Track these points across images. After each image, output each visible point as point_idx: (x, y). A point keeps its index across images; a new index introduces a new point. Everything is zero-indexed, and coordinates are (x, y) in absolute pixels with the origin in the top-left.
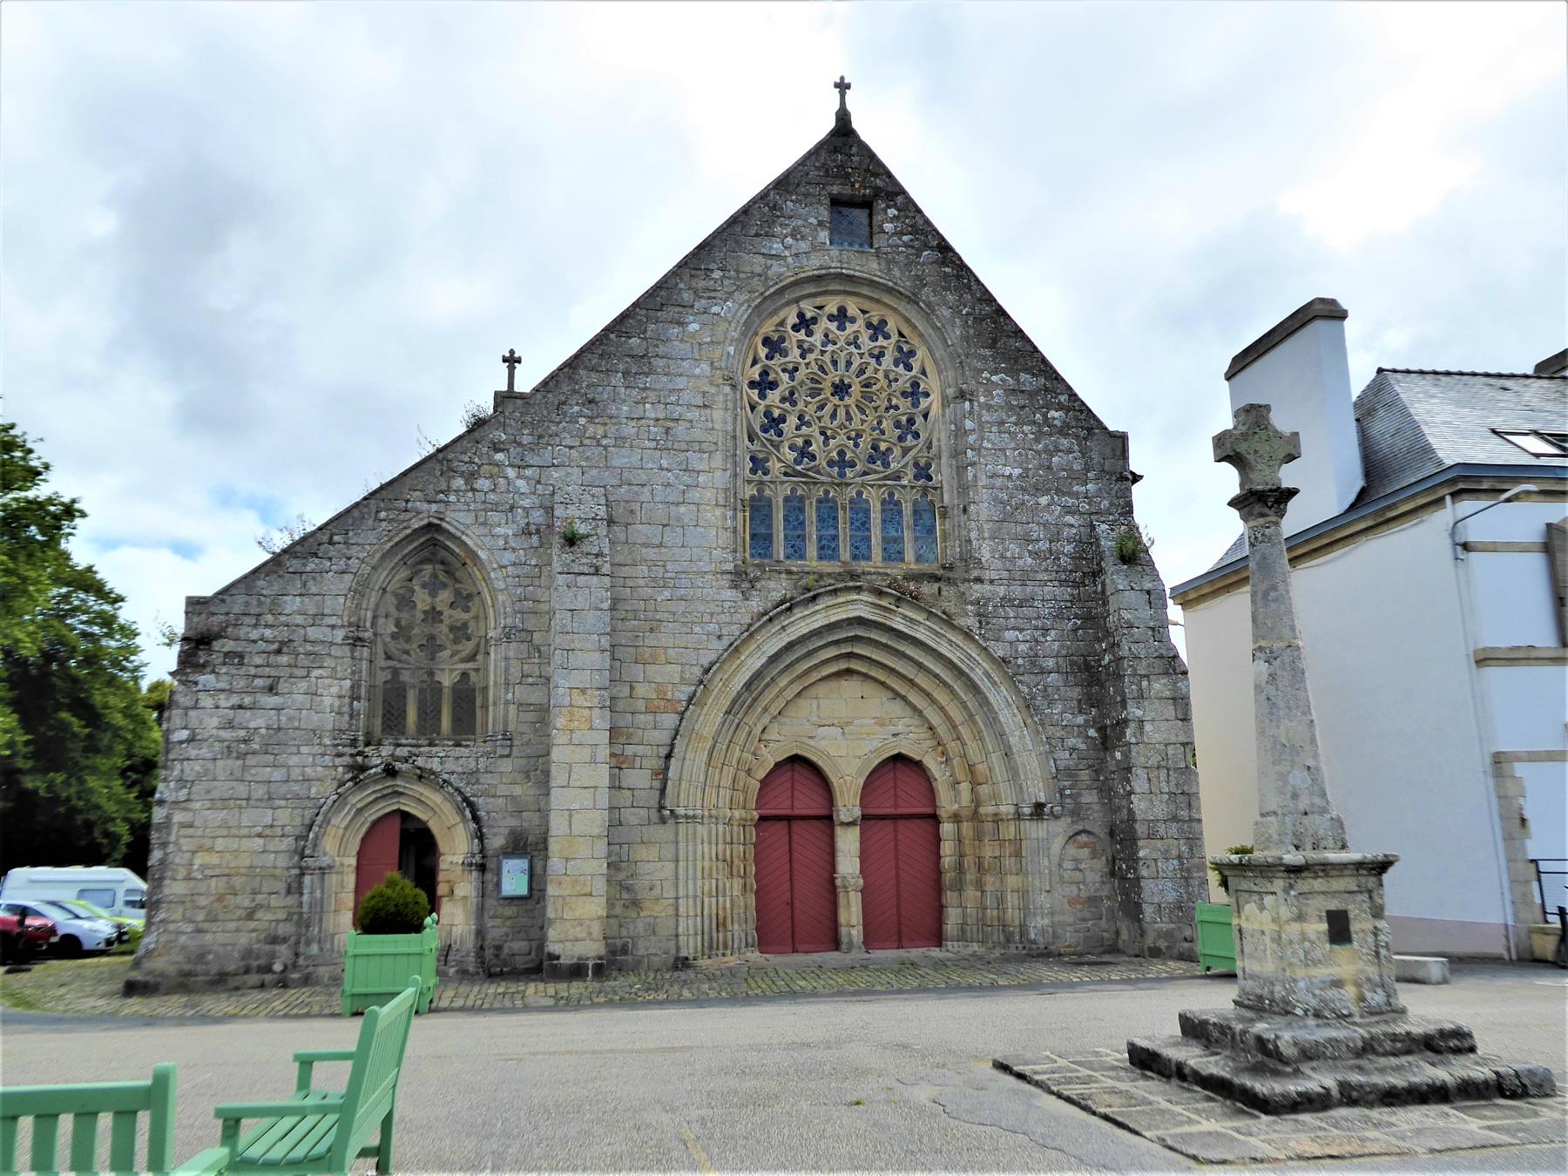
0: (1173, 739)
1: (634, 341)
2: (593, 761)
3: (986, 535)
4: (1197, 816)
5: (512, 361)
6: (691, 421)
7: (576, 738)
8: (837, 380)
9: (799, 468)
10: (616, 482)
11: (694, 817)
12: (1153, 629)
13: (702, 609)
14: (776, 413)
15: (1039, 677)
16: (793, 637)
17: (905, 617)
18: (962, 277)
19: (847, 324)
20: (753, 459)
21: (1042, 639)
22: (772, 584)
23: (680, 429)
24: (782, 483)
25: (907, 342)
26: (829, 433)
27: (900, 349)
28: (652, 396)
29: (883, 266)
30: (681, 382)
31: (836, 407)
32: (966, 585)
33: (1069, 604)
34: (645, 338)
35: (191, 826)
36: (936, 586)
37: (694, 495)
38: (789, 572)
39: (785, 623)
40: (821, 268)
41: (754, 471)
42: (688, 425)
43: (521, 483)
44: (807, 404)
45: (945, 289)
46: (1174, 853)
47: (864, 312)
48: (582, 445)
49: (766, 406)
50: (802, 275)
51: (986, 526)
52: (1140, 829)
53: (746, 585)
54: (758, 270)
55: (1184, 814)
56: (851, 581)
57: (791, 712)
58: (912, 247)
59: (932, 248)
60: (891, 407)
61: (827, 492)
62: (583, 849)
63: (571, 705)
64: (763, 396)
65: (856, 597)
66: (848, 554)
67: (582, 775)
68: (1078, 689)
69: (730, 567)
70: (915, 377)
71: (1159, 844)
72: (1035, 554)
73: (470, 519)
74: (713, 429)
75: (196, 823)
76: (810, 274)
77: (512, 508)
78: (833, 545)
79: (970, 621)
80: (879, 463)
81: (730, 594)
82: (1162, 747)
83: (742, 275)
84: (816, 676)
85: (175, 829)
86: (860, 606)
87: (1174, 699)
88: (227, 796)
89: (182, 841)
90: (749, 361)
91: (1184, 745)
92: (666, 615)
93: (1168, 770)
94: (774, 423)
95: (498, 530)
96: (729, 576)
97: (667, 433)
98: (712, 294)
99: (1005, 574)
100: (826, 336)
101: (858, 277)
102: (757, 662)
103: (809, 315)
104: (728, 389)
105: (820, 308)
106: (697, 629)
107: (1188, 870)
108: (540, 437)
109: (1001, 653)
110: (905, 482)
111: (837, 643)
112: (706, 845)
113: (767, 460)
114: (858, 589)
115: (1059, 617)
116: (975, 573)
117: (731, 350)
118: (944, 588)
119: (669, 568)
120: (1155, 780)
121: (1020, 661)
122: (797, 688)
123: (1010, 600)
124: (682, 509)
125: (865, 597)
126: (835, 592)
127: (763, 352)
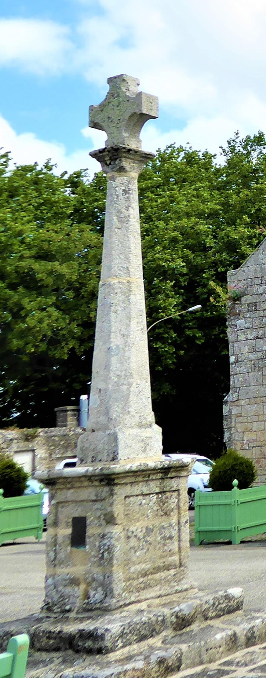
35: (241, 416)
75: (243, 415)
85: (233, 417)
88: (256, 395)
89: (238, 425)
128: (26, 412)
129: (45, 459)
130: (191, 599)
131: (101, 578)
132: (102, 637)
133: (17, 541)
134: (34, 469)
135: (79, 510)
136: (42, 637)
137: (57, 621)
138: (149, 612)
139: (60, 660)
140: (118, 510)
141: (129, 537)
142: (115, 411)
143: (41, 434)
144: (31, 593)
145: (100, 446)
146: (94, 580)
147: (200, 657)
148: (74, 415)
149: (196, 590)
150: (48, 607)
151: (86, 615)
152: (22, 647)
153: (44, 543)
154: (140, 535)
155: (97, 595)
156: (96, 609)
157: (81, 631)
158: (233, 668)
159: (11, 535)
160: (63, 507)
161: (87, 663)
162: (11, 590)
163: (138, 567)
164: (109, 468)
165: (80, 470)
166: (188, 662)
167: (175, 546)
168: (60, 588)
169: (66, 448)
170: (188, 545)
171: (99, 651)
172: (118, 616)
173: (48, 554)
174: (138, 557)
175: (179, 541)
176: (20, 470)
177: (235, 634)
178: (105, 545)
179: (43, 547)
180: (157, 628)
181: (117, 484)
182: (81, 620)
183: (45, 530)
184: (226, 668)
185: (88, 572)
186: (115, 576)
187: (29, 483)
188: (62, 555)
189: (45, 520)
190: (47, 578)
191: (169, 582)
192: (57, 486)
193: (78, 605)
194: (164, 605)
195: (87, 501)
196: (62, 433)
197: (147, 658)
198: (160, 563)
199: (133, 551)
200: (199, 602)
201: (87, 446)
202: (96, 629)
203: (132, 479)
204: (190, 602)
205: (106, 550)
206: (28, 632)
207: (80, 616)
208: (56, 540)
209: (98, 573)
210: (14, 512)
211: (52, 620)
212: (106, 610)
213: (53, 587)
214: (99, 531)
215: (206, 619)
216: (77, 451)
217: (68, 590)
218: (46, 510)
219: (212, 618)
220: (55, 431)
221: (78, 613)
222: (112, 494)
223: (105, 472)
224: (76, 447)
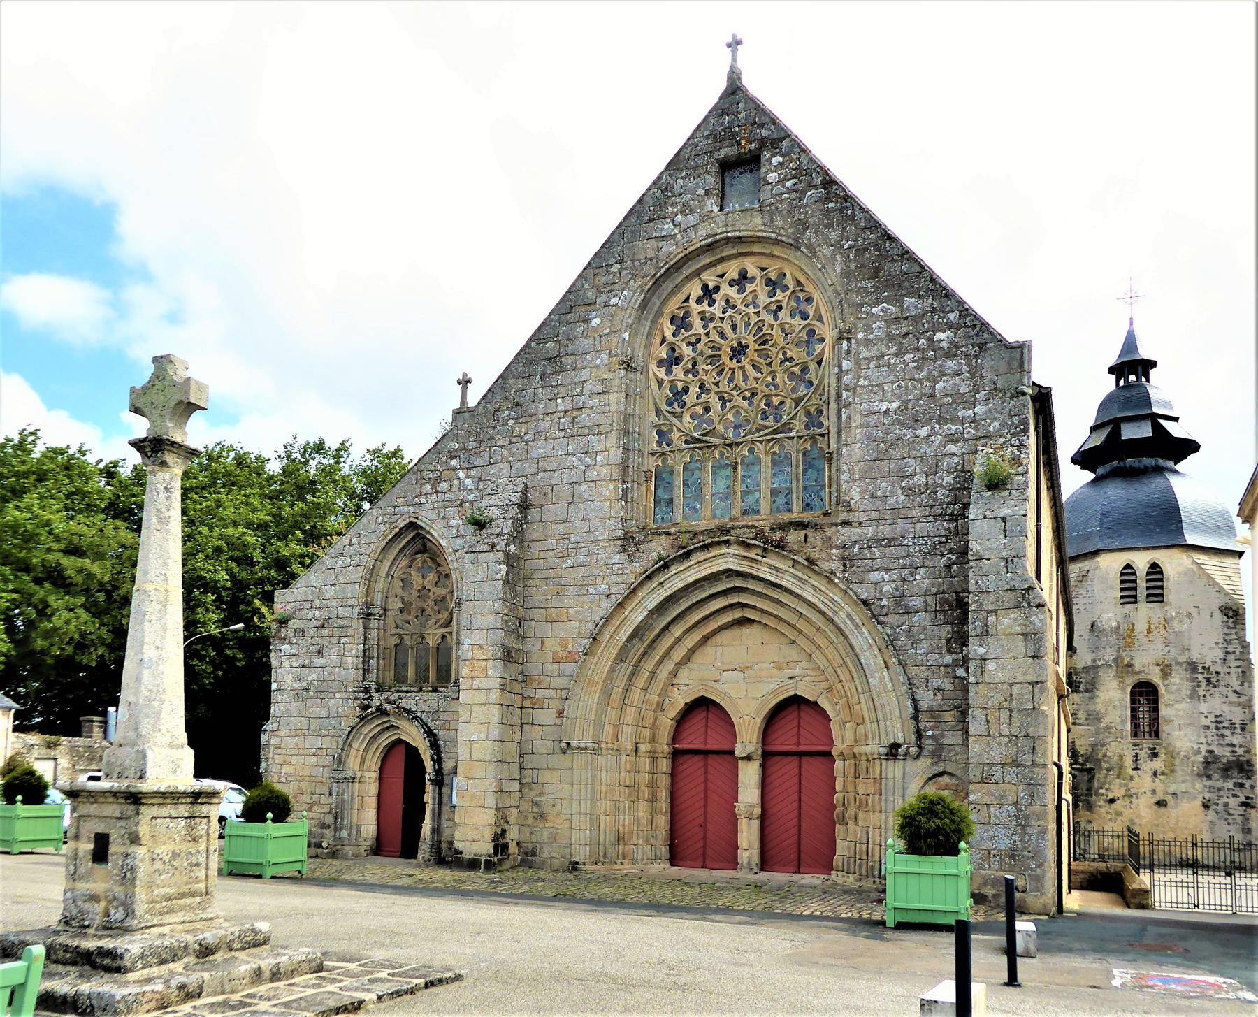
0: (1020, 679)
1: (550, 345)
2: (487, 703)
3: (857, 476)
4: (1042, 761)
5: (465, 382)
6: (592, 408)
7: (476, 682)
9: (695, 435)
10: (534, 471)
11: (586, 748)
12: (1006, 560)
13: (596, 572)
14: (680, 386)
15: (905, 617)
16: (670, 592)
17: (770, 566)
20: (660, 433)
21: (912, 578)
22: (653, 546)
23: (583, 417)
24: (681, 451)
28: (562, 391)
30: (585, 374)
32: (834, 529)
33: (944, 539)
34: (558, 341)
36: (803, 533)
37: (593, 474)
38: (667, 534)
39: (662, 580)
41: (659, 443)
42: (589, 411)
43: (468, 482)
46: (1011, 798)
48: (510, 443)
49: (671, 381)
51: (857, 468)
52: (974, 773)
53: (633, 548)
55: (1027, 758)
56: (721, 536)
57: (697, 657)
62: (479, 771)
63: (472, 658)
64: (669, 372)
65: (723, 551)
67: (479, 714)
68: (949, 628)
69: (619, 533)
71: (993, 788)
72: (909, 491)
73: (434, 516)
74: (609, 412)
77: (462, 502)
79: (836, 566)
80: (771, 418)
81: (617, 558)
82: (1006, 687)
84: (713, 625)
86: (729, 558)
87: (1025, 635)
88: (297, 727)
90: (658, 341)
91: (1033, 684)
92: (568, 580)
93: (1011, 711)
94: (678, 395)
95: (454, 522)
96: (619, 542)
97: (573, 422)
99: (874, 515)
102: (639, 617)
104: (623, 372)
106: (592, 590)
107: (1026, 818)
108: (482, 441)
109: (864, 596)
110: (793, 434)
111: (724, 593)
112: (603, 772)
113: (671, 431)
114: (727, 542)
115: (932, 553)
116: (842, 517)
119: (573, 538)
120: (993, 722)
121: (884, 602)
122: (696, 637)
123: (878, 540)
124: (584, 487)
125: (735, 550)
126: (706, 547)
127: (669, 330)
128: (49, 717)
129: (68, 769)
130: (216, 928)
131: (123, 897)
132: (121, 957)
133: (34, 850)
134: (55, 779)
135: (102, 825)
136: (58, 950)
137: (74, 936)
138: (172, 937)
139: (77, 974)
140: (144, 830)
141: (153, 860)
142: (145, 727)
143: (65, 743)
144: (48, 904)
145: (127, 763)
146: (115, 898)
147: (222, 986)
148: (101, 727)
149: (222, 920)
150: (66, 921)
151: (106, 932)
152: (37, 957)
153: (64, 855)
154: (166, 859)
155: (117, 914)
156: (116, 928)
157: (99, 948)
158: (256, 1001)
159: (29, 844)
160: (85, 821)
161: (104, 980)
162: (27, 900)
163: (163, 891)
164: (135, 787)
165: (104, 785)
166: (210, 990)
167: (202, 874)
168: (79, 903)
169: (91, 760)
170: (216, 874)
171: (118, 970)
172: (139, 937)
173: (67, 868)
174: (163, 880)
175: (207, 869)
176: (40, 778)
177: (259, 968)
178: (128, 864)
179: (63, 860)
180: (180, 953)
181: (143, 804)
182: (101, 937)
183: (65, 843)
184: (249, 1000)
185: (110, 890)
186: (137, 897)
187: (48, 792)
188: (82, 870)
189: (65, 833)
190: (65, 891)
191: (194, 909)
192: (80, 799)
193: (97, 922)
194: (188, 932)
195: (111, 817)
196: (86, 744)
197: (167, 982)
198: (185, 889)
199: (157, 874)
200: (224, 932)
201: (114, 760)
202: (115, 948)
203: (160, 801)
204: (215, 932)
205: (129, 870)
206: (44, 943)
207: (99, 933)
208: (76, 854)
209: (119, 892)
210: (33, 820)
211: (70, 934)
212: (127, 930)
213: (71, 901)
214: (122, 849)
215: (231, 950)
216: (103, 765)
217: (88, 906)
218: (67, 822)
219: (236, 950)
220: (79, 741)
221: (97, 929)
222: (138, 814)
223: (132, 790)
224: (101, 760)
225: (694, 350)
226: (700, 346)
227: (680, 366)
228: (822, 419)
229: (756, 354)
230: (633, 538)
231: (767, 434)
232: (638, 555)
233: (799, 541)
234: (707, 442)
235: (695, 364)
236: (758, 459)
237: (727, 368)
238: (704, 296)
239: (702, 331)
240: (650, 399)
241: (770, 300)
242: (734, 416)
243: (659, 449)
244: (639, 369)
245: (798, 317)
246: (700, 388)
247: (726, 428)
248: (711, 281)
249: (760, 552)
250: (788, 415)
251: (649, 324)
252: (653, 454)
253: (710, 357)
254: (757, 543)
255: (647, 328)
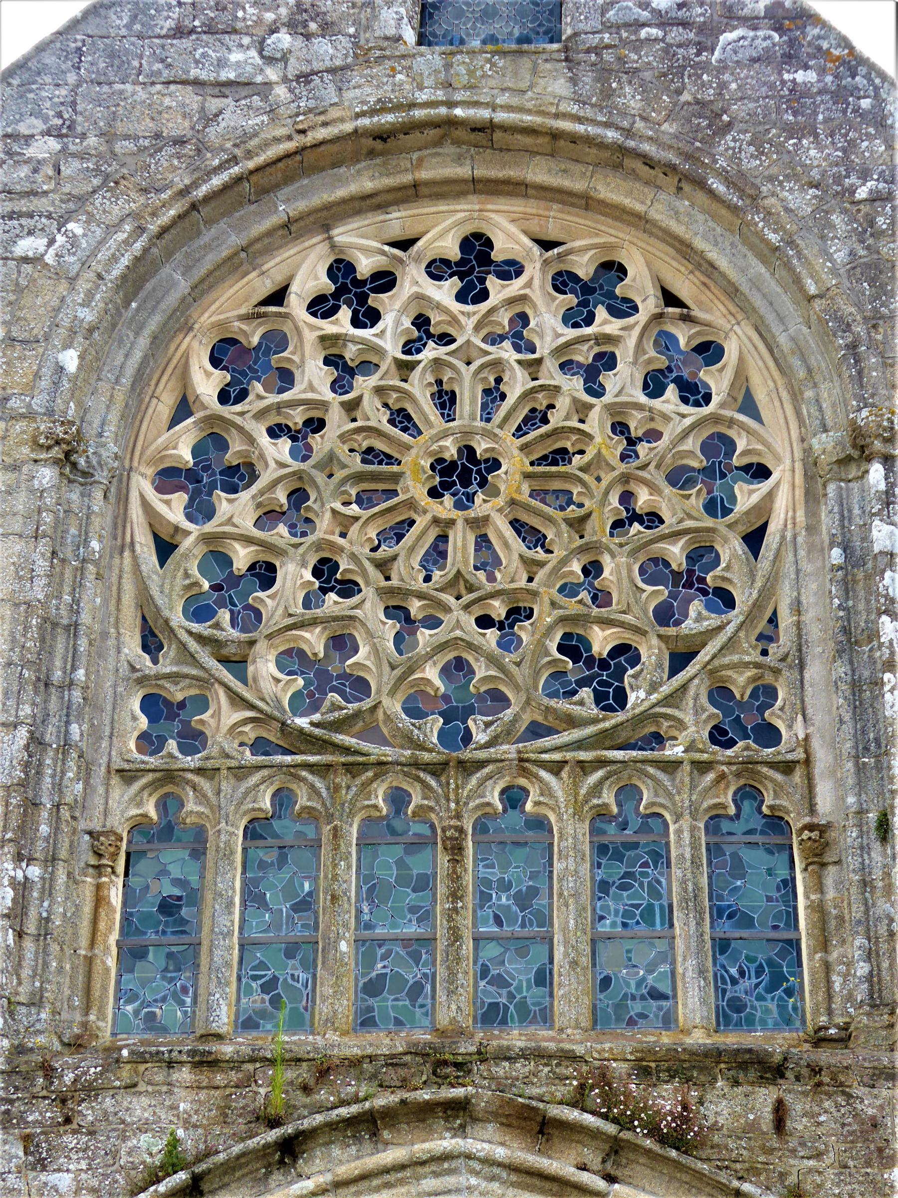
8: (451, 450)
9: (302, 722)
18: (854, 91)
19: (492, 283)
20: (151, 704)
24: (241, 772)
25: (687, 319)
26: (415, 607)
27: (666, 342)
29: (588, 79)
31: (444, 526)
40: (381, 108)
44: (344, 524)
45: (792, 131)
47: (547, 245)
49: (207, 538)
50: (322, 134)
54: (177, 126)
58: (685, 24)
59: (752, 22)
60: (635, 517)
61: (398, 799)
66: (464, 998)
70: (715, 419)
76: (348, 127)
78: (412, 975)
83: (122, 146)
90: (164, 407)
98: (23, 205)
100: (421, 322)
101: (505, 128)
103: (365, 266)
104: (47, 475)
105: (405, 244)
110: (675, 751)
113: (202, 704)
117: (70, 360)
118: (797, 1106)
225: (303, 453)
226: (320, 443)
227: (245, 496)
228: (773, 716)
229: (526, 488)
230: (48, 1071)
231: (579, 745)
232: (70, 1141)
233: (752, 1127)
234: (346, 750)
235: (298, 496)
236: (540, 824)
237: (421, 522)
238: (336, 295)
239: (393, 349)
240: (128, 586)
241: (571, 333)
242: (445, 672)
243: (153, 761)
244: (102, 476)
245: (671, 392)
246: (316, 573)
247: (412, 711)
248: (365, 250)
249: (593, 1158)
250: (653, 687)
251: (143, 342)
252: (127, 776)
253: (358, 477)
254: (589, 1119)
255: (138, 355)
